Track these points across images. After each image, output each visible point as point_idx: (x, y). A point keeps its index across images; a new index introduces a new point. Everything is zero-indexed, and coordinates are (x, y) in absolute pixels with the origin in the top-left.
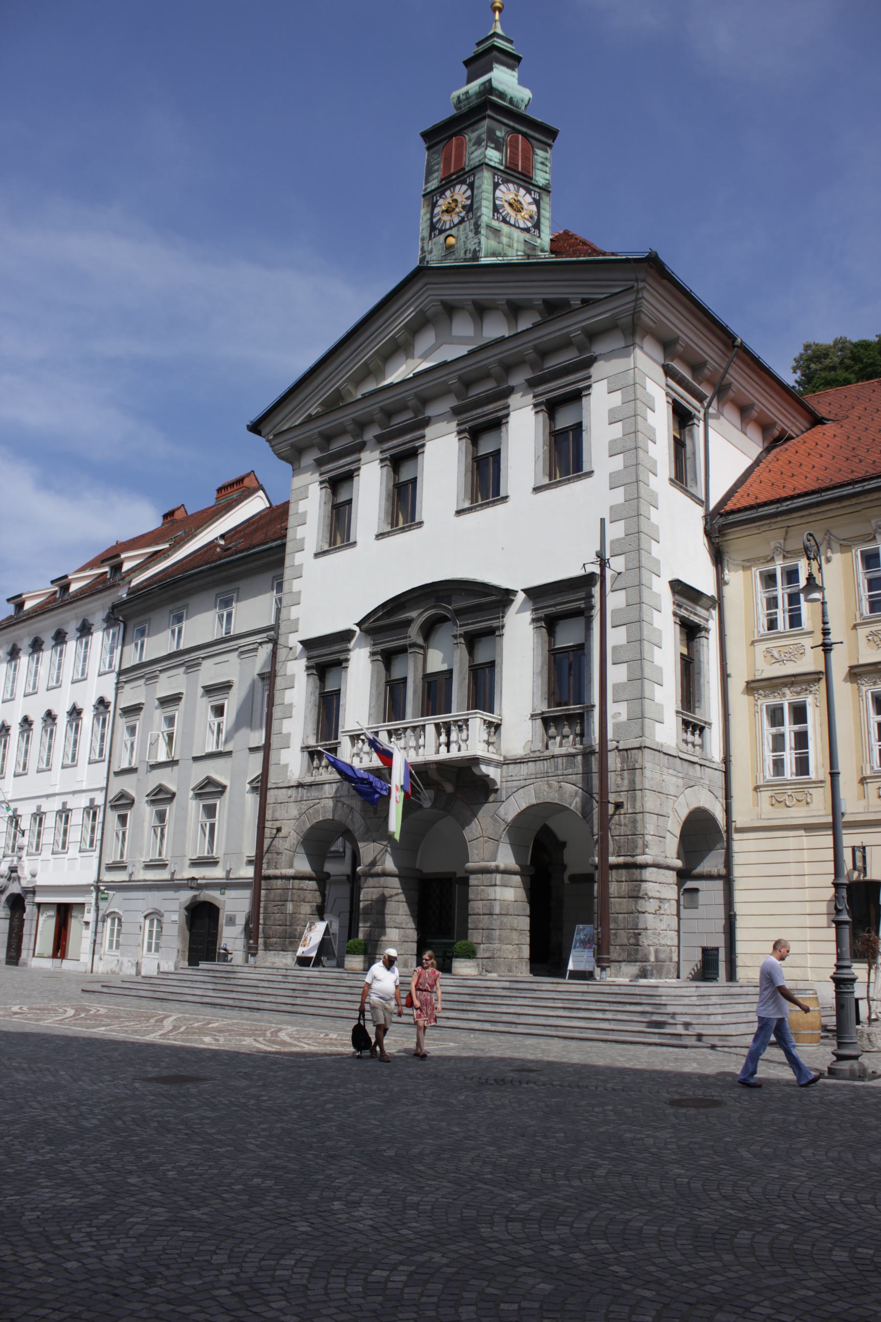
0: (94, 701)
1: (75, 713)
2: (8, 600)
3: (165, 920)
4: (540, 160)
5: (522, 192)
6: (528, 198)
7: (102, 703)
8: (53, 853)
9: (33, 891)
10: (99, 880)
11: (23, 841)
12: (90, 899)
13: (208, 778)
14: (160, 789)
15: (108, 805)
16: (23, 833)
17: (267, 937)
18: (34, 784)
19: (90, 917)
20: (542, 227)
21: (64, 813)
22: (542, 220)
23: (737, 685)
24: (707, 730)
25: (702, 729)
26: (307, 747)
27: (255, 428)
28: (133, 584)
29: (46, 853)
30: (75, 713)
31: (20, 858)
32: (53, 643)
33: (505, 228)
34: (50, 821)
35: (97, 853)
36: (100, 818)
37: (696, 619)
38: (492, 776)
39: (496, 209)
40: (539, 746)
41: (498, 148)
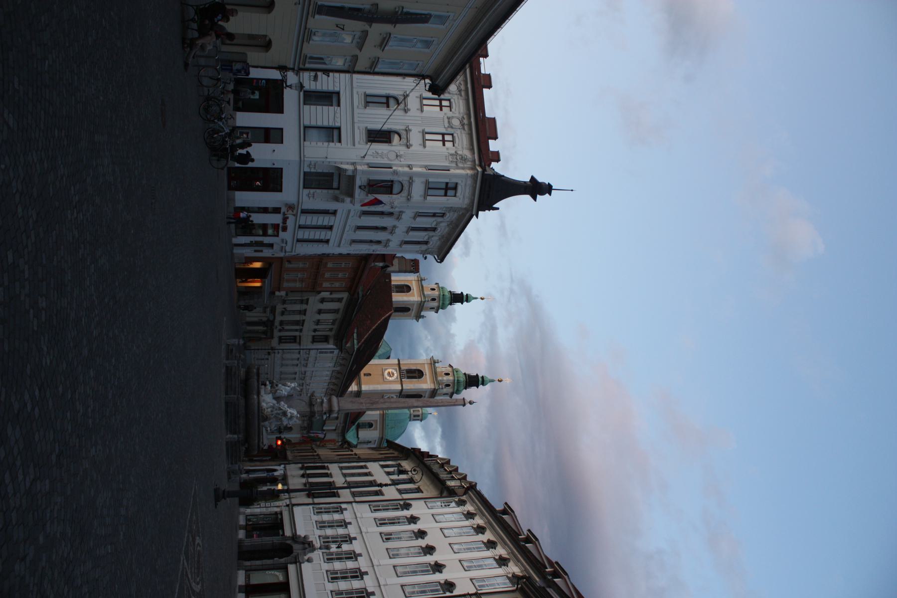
1: (438, 567)
2: (506, 503)
7: (449, 585)
8: (327, 571)
11: (334, 548)
16: (339, 547)
18: (378, 547)
28: (548, 590)
29: (326, 566)
31: (320, 548)
32: (485, 541)
34: (350, 565)
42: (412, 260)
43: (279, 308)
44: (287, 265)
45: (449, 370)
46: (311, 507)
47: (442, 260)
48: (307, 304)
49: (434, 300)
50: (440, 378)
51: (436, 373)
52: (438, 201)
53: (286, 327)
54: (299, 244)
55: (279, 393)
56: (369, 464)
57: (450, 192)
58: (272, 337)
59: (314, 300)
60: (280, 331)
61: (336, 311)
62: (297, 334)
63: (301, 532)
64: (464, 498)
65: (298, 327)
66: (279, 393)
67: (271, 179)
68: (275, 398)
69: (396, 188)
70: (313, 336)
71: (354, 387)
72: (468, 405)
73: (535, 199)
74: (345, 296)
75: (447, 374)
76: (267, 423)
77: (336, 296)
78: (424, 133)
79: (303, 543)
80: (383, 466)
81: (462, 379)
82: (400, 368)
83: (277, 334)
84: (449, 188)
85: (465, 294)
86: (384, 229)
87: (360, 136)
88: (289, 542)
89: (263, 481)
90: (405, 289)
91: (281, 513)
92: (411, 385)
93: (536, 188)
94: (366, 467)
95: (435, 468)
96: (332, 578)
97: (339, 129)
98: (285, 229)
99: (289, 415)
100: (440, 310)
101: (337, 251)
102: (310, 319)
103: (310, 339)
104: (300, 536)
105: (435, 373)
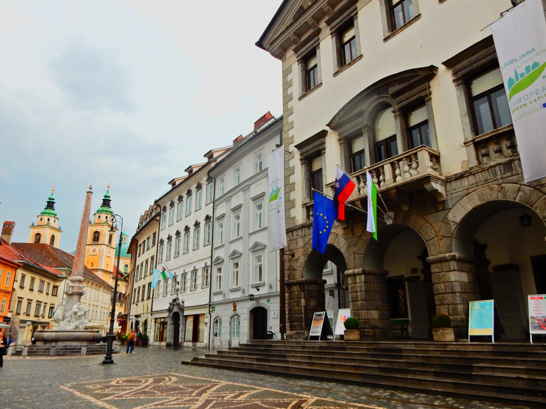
0: (204, 217)
1: (197, 225)
2: (169, 183)
3: (241, 318)
7: (208, 218)
8: (191, 291)
11: (178, 287)
12: (205, 311)
13: (256, 242)
14: (234, 253)
15: (213, 264)
17: (291, 321)
18: (183, 259)
19: (207, 320)
21: (195, 271)
26: (305, 204)
27: (260, 44)
29: (188, 291)
34: (189, 276)
35: (209, 289)
36: (209, 272)
40: (474, 163)
42: (4, 226)
43: (23, 317)
45: (97, 215)
46: (154, 300)
48: (22, 298)
49: (49, 220)
50: (101, 222)
51: (98, 223)
53: (41, 313)
55: (60, 317)
56: (137, 264)
58: (48, 323)
59: (19, 293)
60: (43, 317)
61: (33, 279)
62: (48, 307)
63: (167, 307)
64: (162, 208)
65: (43, 305)
66: (60, 317)
68: (63, 320)
70: (52, 295)
71: (99, 274)
72: (91, 190)
74: (20, 272)
75: (99, 217)
76: (81, 326)
77: (19, 278)
79: (173, 305)
80: (139, 256)
81: (105, 209)
82: (91, 245)
83: (46, 320)
85: (48, 200)
88: (171, 315)
89: (137, 329)
91: (156, 319)
94: (138, 266)
95: (144, 224)
96: (195, 288)
99: (77, 310)
100: (57, 217)
102: (35, 296)
104: (169, 307)
105: (98, 224)
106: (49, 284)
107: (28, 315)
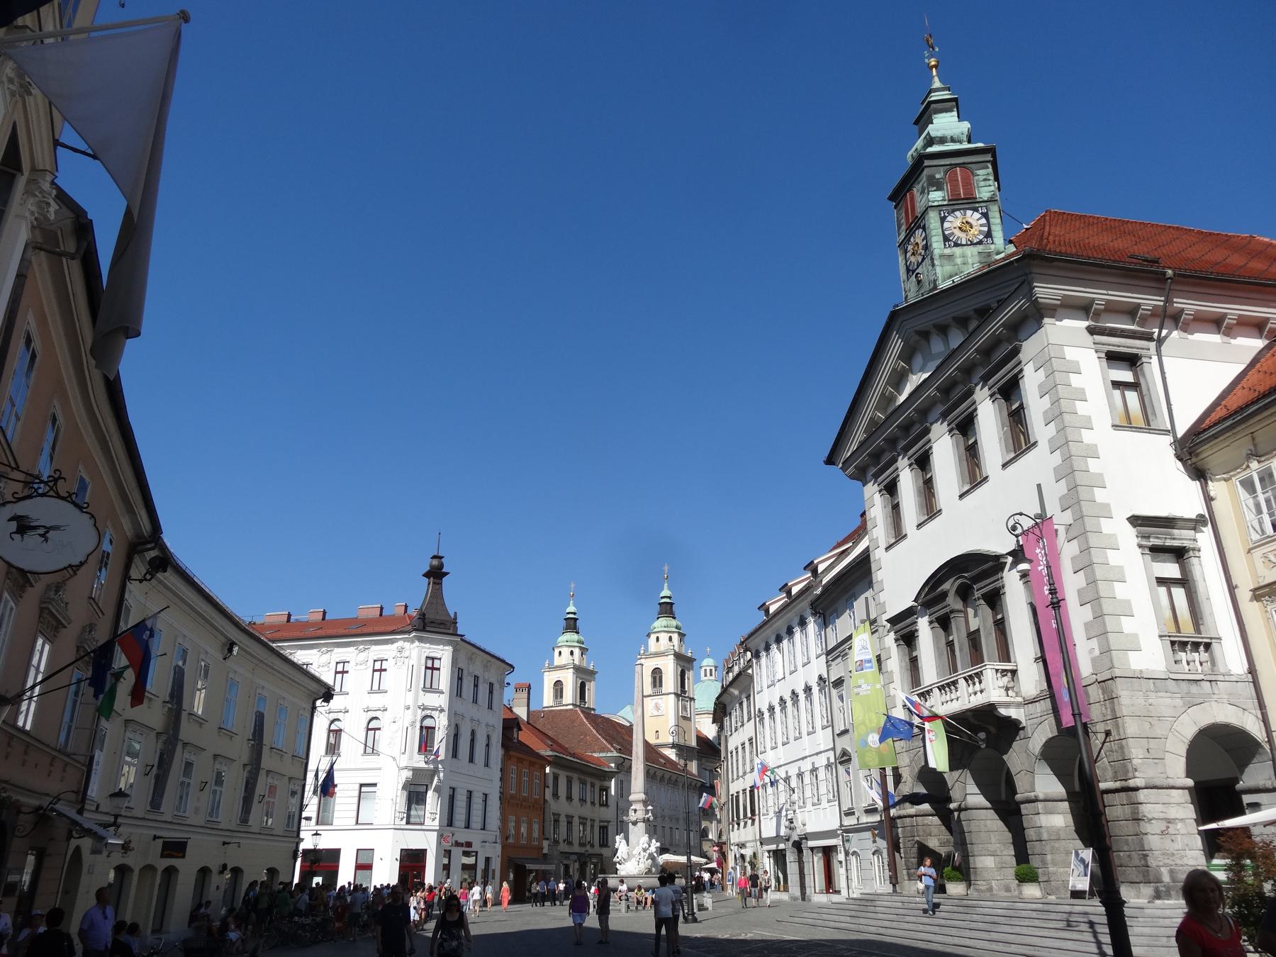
1: (808, 689)
4: (982, 178)
5: (969, 213)
6: (977, 215)
9: (806, 837)
10: (841, 825)
11: (795, 797)
19: (841, 857)
20: (994, 234)
22: (993, 227)
23: (1244, 595)
24: (1215, 646)
25: (1208, 646)
27: (830, 461)
29: (809, 806)
30: (808, 689)
33: (957, 251)
37: (1176, 543)
38: (1014, 716)
39: (946, 239)
41: (939, 188)
43: (563, 847)
44: (511, 841)
47: (512, 666)
49: (572, 653)
50: (662, 649)
52: (444, 678)
54: (488, 826)
57: (437, 664)
59: (554, 806)
60: (592, 846)
61: (569, 781)
67: (412, 861)
69: (428, 723)
73: (447, 574)
75: (658, 639)
78: (372, 692)
83: (597, 849)
84: (431, 667)
86: (473, 733)
87: (371, 761)
90: (558, 685)
92: (670, 683)
93: (436, 574)
97: (361, 785)
98: (469, 844)
101: (497, 784)
102: (576, 809)
103: (603, 809)
106: (593, 786)
107: (570, 843)
